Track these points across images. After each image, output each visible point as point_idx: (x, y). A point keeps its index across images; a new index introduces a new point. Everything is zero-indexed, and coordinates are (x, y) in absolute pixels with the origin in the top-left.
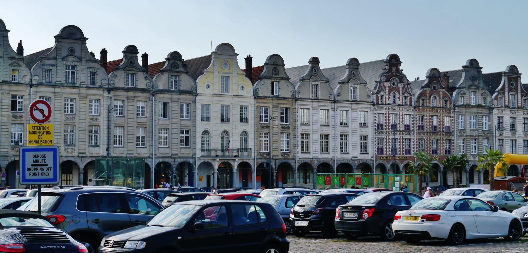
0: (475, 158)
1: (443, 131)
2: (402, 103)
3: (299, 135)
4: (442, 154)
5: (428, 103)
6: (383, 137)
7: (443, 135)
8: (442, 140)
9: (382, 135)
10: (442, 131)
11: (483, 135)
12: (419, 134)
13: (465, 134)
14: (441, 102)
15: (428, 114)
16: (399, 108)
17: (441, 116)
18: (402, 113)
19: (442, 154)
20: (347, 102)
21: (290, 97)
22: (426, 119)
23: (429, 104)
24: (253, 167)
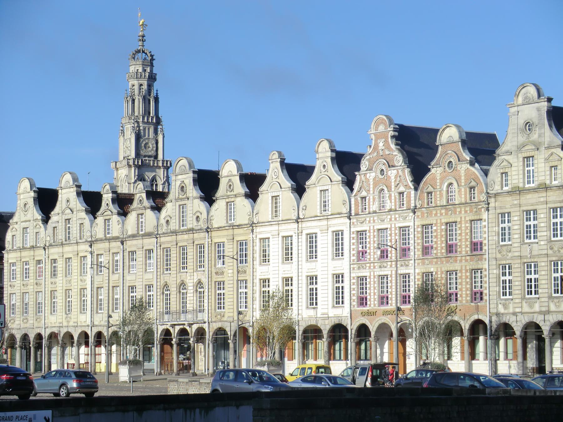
0: (531, 307)
1: (467, 252)
2: (395, 206)
3: (257, 281)
4: (464, 302)
5: (438, 199)
6: (385, 273)
7: (466, 261)
8: (464, 271)
9: (364, 271)
10: (464, 253)
11: (550, 252)
12: (424, 264)
13: (510, 255)
14: (463, 193)
15: (439, 221)
16: (389, 217)
17: (463, 222)
18: (395, 224)
19: (464, 302)
20: (316, 218)
21: (246, 222)
22: (436, 231)
23: (440, 201)
24: (229, 333)
